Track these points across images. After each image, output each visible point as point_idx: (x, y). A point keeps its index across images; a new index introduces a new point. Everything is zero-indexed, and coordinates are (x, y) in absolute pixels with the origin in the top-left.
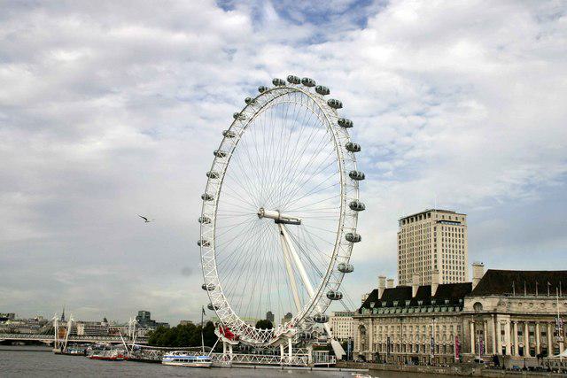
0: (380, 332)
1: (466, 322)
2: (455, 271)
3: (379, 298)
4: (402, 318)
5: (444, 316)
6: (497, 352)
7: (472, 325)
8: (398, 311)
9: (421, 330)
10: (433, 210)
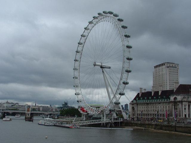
0: (141, 109)
1: (171, 105)
2: (172, 83)
3: (140, 96)
5: (163, 103)
6: (182, 116)
7: (173, 106)
8: (146, 101)
9: (155, 109)
10: (166, 63)
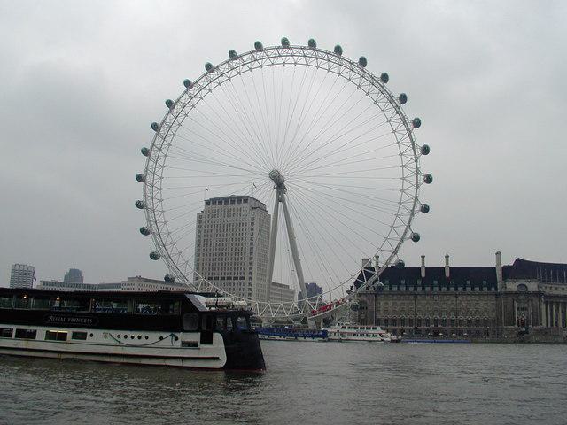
1: (510, 299)
4: (416, 296)
